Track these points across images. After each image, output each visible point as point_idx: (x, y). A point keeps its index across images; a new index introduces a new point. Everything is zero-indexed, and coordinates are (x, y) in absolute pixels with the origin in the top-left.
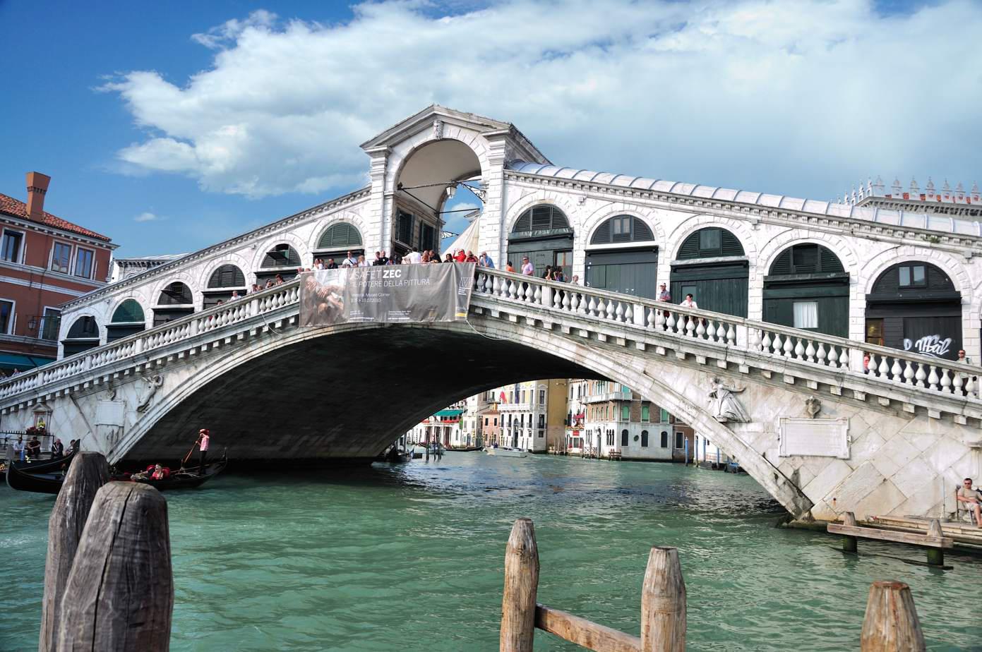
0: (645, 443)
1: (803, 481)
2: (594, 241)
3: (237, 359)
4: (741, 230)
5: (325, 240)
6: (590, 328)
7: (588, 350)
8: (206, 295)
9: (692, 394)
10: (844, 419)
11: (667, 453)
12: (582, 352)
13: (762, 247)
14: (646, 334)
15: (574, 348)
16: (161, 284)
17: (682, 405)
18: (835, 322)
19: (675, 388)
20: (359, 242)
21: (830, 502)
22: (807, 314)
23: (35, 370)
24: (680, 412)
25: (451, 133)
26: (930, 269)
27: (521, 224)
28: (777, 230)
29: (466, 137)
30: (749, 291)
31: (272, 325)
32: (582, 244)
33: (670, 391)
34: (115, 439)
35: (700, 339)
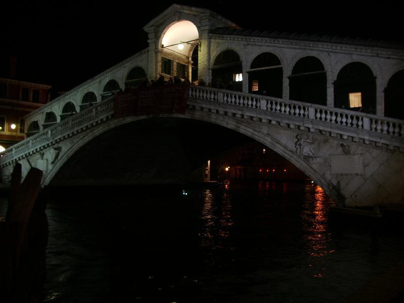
1: (343, 185)
2: (252, 67)
4: (323, 57)
6: (240, 113)
7: (240, 123)
8: (81, 107)
10: (361, 154)
12: (238, 125)
15: (234, 123)
17: (285, 150)
19: (282, 141)
21: (354, 197)
22: (355, 100)
23: (11, 147)
24: (284, 153)
30: (328, 89)
31: (102, 120)
33: (279, 143)
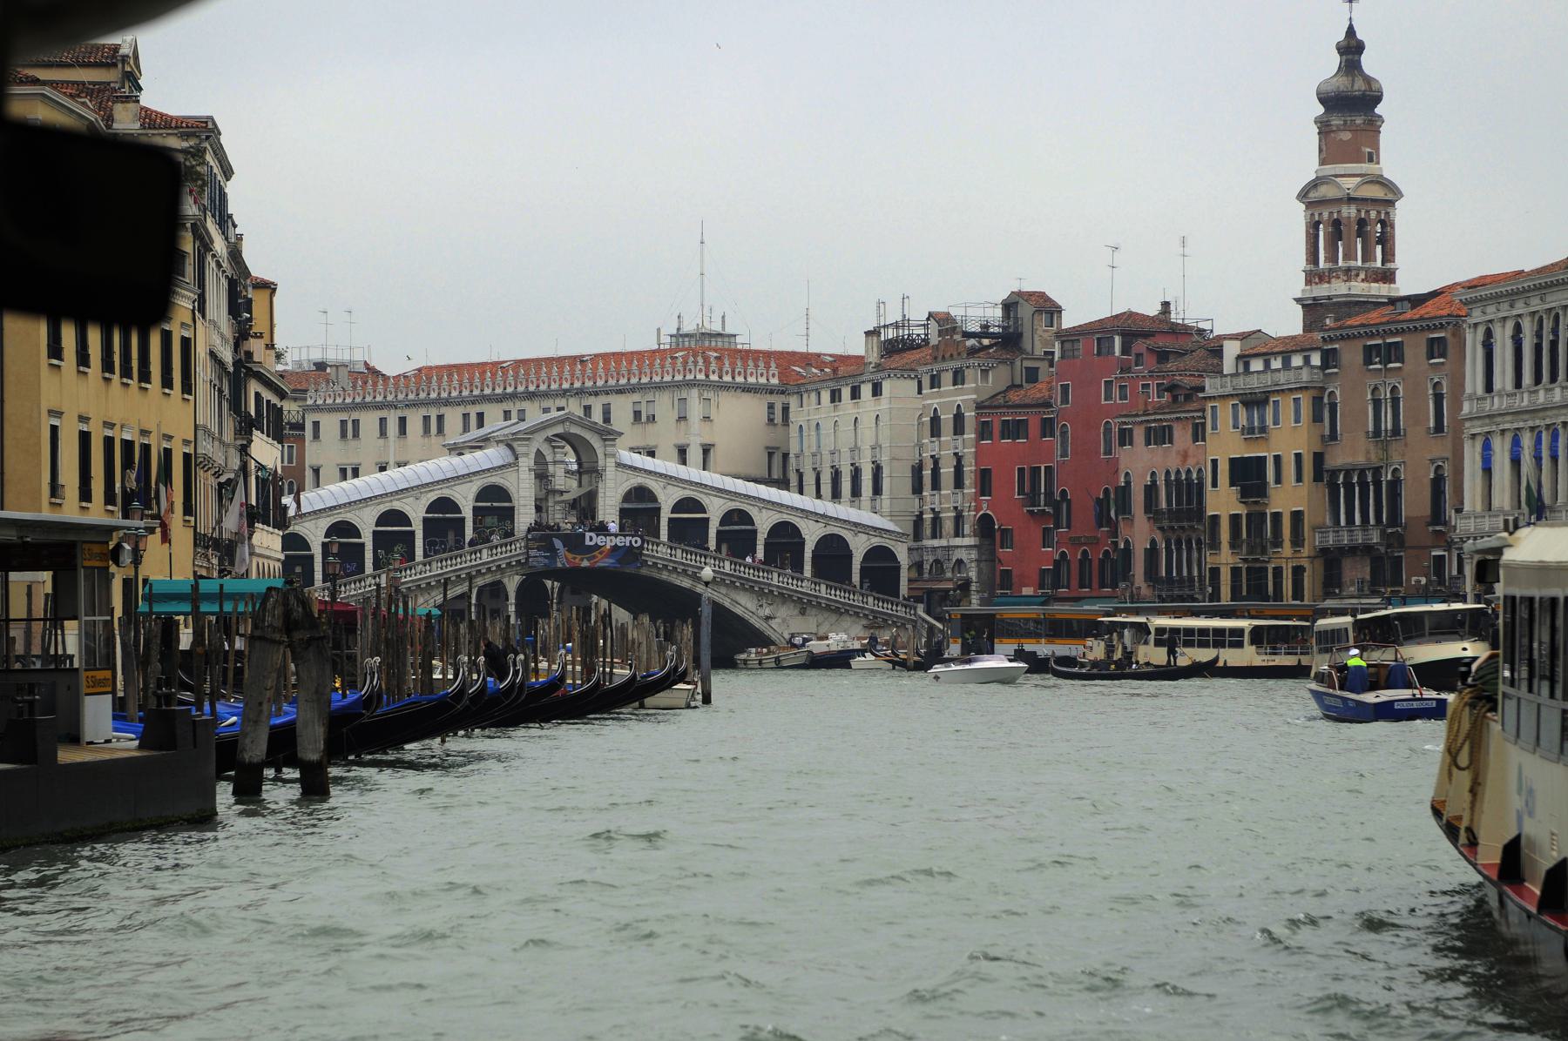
4: (753, 512)
9: (749, 605)
16: (325, 523)
18: (798, 566)
25: (575, 430)
27: (627, 497)
29: (588, 435)
32: (666, 515)
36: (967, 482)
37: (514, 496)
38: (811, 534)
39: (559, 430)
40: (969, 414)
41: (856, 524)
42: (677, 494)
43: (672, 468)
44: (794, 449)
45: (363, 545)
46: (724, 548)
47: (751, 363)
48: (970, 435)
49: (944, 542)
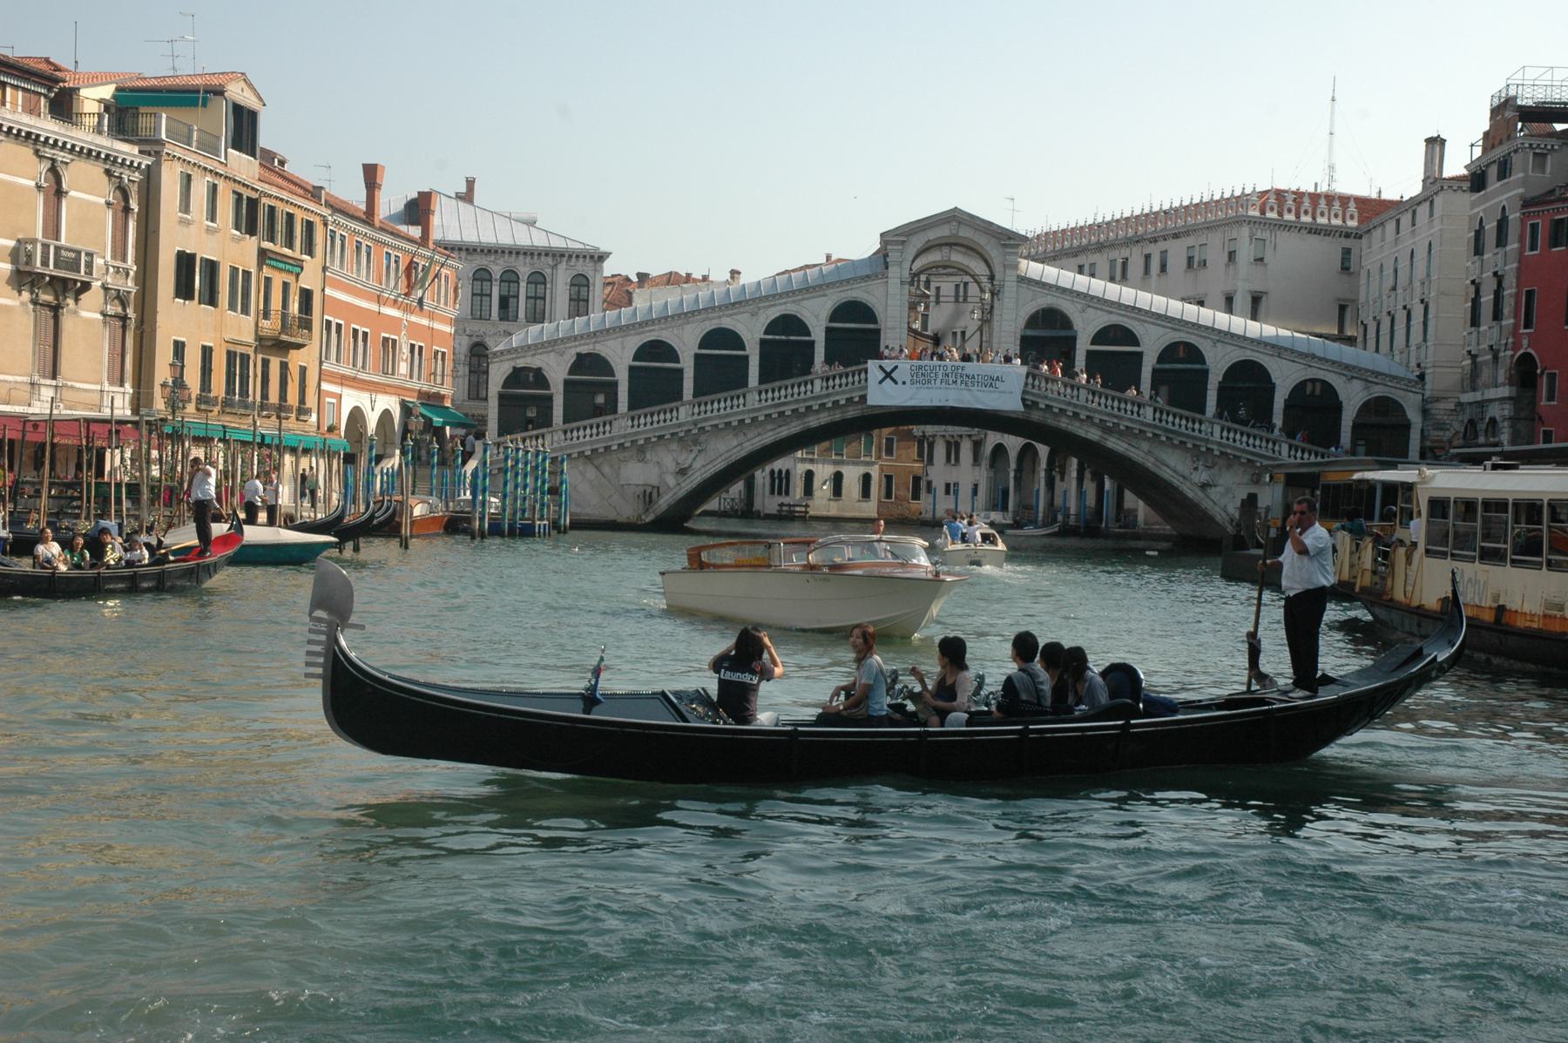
0: (837, 490)
3: (794, 428)
4: (1206, 348)
5: (836, 315)
9: (1180, 468)
11: (870, 509)
13: (1218, 363)
14: (1156, 427)
16: (634, 342)
18: (1262, 416)
20: (875, 321)
25: (965, 233)
26: (1324, 382)
27: (1033, 321)
28: (1230, 348)
34: (648, 497)
35: (1190, 432)
36: (1506, 311)
37: (880, 315)
38: (1285, 378)
39: (943, 232)
40: (1514, 216)
41: (1347, 367)
42: (1100, 320)
43: (1222, 320)
44: (1362, 299)
45: (681, 371)
46: (1164, 389)
47: (1323, 202)
48: (1513, 246)
49: (1478, 396)
